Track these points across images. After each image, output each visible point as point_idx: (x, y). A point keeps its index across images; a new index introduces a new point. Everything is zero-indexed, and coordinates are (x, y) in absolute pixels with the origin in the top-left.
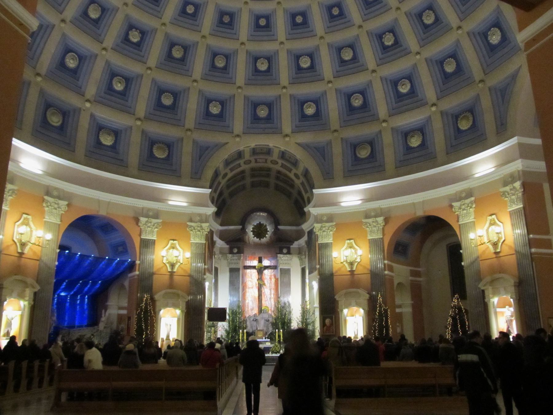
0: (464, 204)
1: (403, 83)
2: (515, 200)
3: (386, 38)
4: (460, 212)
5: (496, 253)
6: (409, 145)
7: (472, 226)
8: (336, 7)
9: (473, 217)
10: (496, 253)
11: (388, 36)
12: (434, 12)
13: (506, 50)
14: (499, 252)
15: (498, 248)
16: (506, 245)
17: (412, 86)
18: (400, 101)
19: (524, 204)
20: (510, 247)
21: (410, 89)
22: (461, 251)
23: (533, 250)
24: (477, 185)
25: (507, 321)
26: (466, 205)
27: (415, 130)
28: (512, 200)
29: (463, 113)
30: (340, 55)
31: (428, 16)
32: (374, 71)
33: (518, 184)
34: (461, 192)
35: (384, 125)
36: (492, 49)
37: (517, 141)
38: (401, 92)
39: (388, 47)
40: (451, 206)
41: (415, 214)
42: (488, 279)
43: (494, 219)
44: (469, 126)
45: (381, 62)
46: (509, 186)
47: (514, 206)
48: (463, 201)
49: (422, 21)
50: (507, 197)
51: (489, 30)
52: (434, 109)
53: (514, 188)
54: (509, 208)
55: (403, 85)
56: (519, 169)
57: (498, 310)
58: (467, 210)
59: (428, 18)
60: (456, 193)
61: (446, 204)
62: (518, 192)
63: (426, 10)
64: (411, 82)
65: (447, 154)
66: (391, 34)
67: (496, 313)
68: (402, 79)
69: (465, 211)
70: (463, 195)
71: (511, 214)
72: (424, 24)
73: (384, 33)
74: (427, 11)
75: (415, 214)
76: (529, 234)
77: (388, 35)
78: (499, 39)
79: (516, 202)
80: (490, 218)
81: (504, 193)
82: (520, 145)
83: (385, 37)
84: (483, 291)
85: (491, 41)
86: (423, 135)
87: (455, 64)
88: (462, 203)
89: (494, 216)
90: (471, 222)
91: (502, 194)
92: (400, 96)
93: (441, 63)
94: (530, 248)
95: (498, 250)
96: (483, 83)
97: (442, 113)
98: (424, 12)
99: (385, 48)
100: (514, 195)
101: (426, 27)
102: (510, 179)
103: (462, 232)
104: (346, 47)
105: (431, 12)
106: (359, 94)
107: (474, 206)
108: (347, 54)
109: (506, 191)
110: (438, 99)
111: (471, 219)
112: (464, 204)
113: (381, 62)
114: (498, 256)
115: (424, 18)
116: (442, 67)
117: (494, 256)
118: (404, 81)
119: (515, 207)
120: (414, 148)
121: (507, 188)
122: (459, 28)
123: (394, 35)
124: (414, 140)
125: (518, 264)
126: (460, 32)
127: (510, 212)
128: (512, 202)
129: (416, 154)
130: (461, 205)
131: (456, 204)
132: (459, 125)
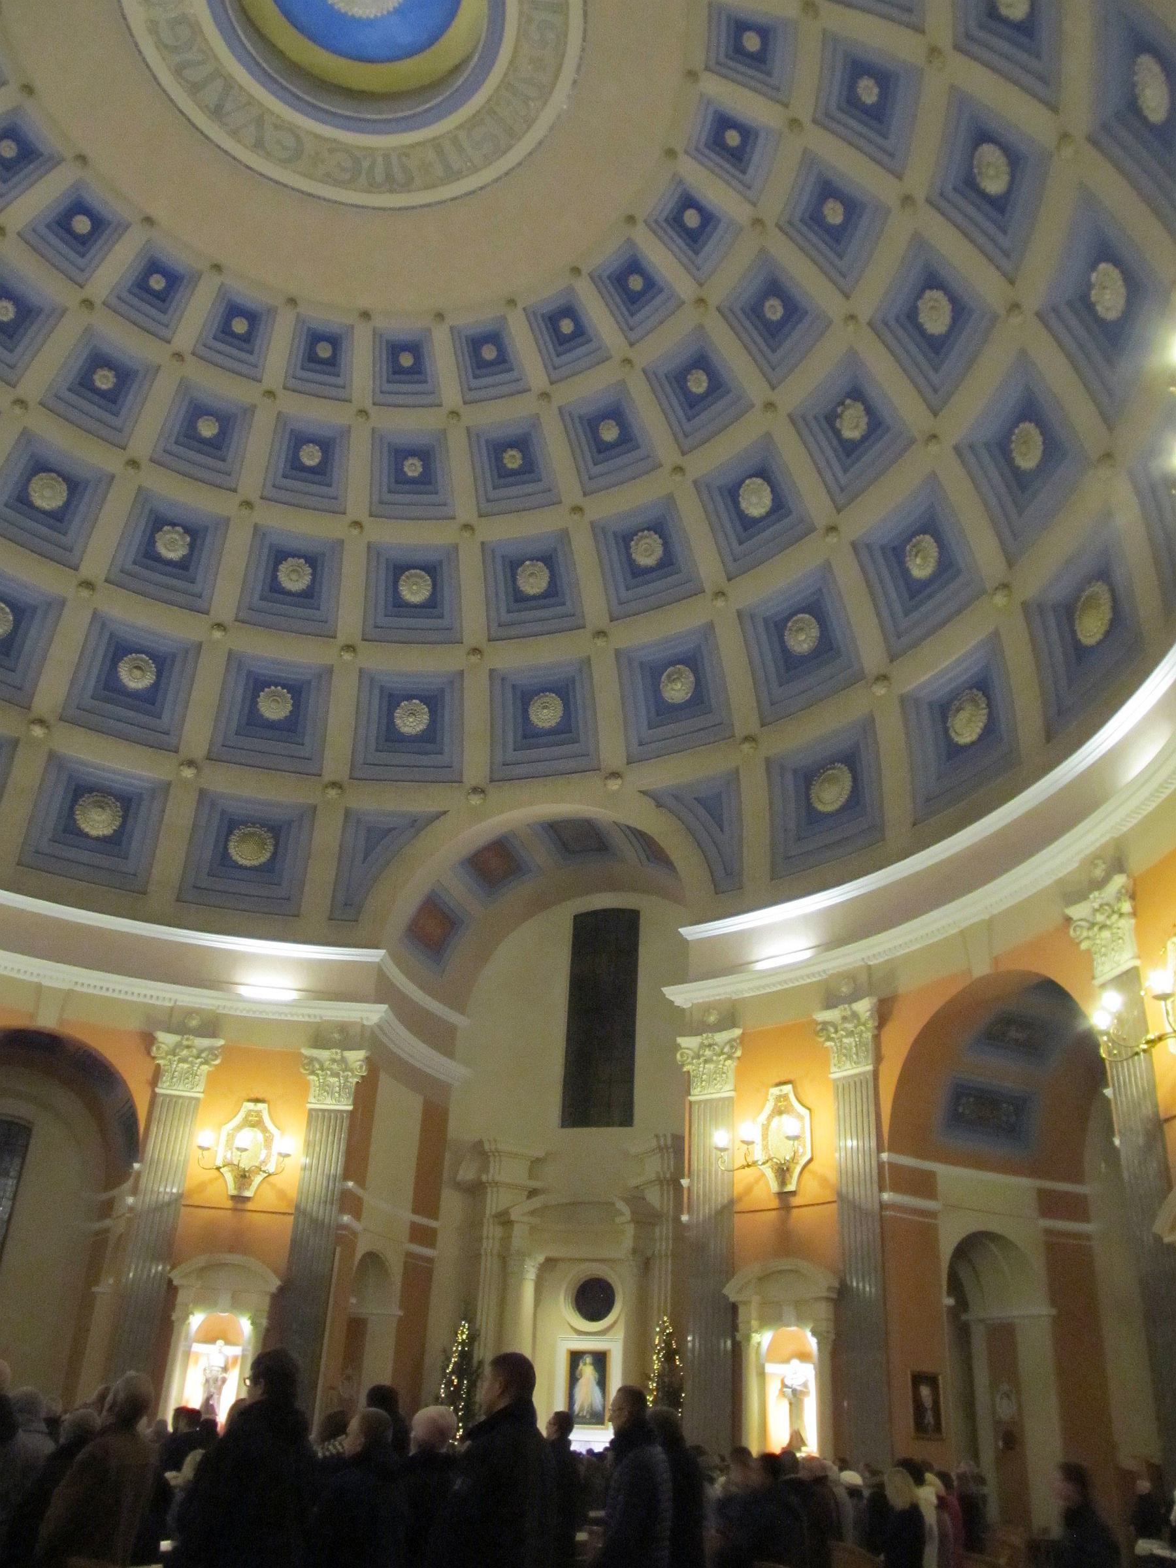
0: (188, 1047)
1: (141, 664)
2: (337, 1089)
3: (168, 536)
4: (171, 1062)
5: (239, 1199)
6: (75, 820)
7: (186, 1108)
8: (113, 372)
9: (201, 1088)
10: (239, 1199)
11: (176, 536)
12: (314, 574)
13: (425, 760)
14: (248, 1199)
15: (248, 1189)
16: (273, 1186)
17: (156, 686)
18: (106, 700)
19: (355, 1104)
20: (282, 1194)
21: (147, 690)
22: (136, 1166)
23: (346, 1218)
24: (238, 1013)
25: (207, 1381)
26: (195, 1051)
27: (111, 794)
28: (328, 1085)
29: (254, 824)
30: (29, 480)
31: (293, 571)
32: (88, 585)
33: (356, 1057)
34: (190, 1012)
35: (38, 731)
36: (391, 737)
37: (377, 960)
38: (118, 679)
39: (158, 559)
40: (148, 1040)
41: (32, 1016)
42: (201, 1260)
43: (259, 1113)
44: (256, 863)
45: (119, 580)
46: (334, 1051)
47: (329, 1101)
48: (191, 1037)
49: (275, 570)
50: (317, 1075)
51: (409, 698)
52: (188, 773)
53: (343, 1060)
54: (313, 1100)
55: (138, 668)
56: (365, 1023)
57: (197, 1347)
58: (192, 1064)
59: (294, 576)
60: (172, 1009)
61: (135, 1024)
62: (350, 1074)
63: (299, 557)
64: (159, 674)
65: (178, 900)
66: (188, 539)
67: (187, 1354)
68: (142, 652)
69: (186, 1066)
70: (194, 1023)
71: (315, 1117)
72: (274, 578)
73: (174, 525)
74: (302, 561)
75: (32, 1016)
76: (346, 1176)
77: (177, 532)
78: (418, 729)
79: (337, 1095)
80: (251, 1106)
81: (312, 1060)
82: (379, 971)
83: (169, 532)
84: (172, 1290)
85: (398, 722)
86: (125, 818)
87: (289, 707)
88: (185, 1043)
89: (260, 1106)
90: (192, 1098)
91: (306, 1061)
92: (111, 687)
93: (258, 684)
94: (342, 1210)
95: (247, 1194)
96: (339, 791)
97: (202, 793)
98: (293, 556)
99: (149, 556)
100: (337, 1075)
101: (274, 588)
102: (336, 1036)
103: (156, 1114)
104: (60, 474)
105: (309, 570)
106: (7, 610)
107: (217, 1062)
108: (47, 493)
109: (316, 1059)
110: (209, 758)
111: (197, 1092)
112: (188, 1047)
113: (119, 580)
114: (240, 1206)
115: (283, 567)
116: (255, 697)
117: (229, 1204)
118: (142, 660)
119: (330, 1104)
120: (87, 836)
121: (324, 1055)
122: (350, 648)
123: (192, 546)
124: (97, 818)
125: (294, 1242)
126: (347, 657)
127: (311, 1110)
128: (325, 1088)
129: (85, 856)
130: (179, 1045)
131: (166, 1039)
132: (231, 844)
